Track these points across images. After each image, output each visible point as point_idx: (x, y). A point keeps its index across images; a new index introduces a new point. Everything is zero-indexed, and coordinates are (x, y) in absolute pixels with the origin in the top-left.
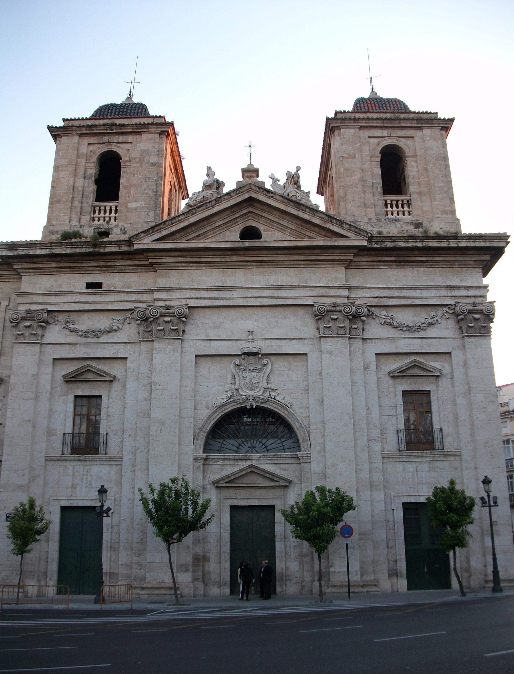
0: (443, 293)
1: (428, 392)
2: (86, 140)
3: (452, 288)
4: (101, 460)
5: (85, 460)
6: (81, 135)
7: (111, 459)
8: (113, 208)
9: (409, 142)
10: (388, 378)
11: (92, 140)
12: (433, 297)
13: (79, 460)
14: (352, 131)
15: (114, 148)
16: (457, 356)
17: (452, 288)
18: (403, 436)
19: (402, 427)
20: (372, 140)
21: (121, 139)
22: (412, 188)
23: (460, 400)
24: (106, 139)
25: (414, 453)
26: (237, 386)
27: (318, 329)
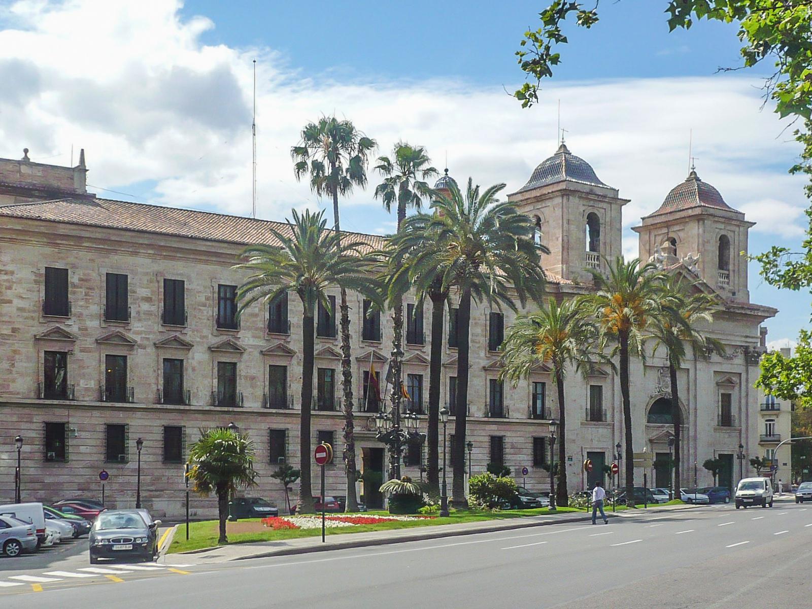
0: (743, 339)
1: (730, 395)
2: (582, 202)
3: (747, 337)
4: (604, 425)
5: (597, 425)
6: (580, 197)
7: (609, 425)
8: (596, 257)
9: (732, 234)
10: (715, 385)
11: (585, 203)
12: (739, 341)
13: (595, 425)
14: (710, 222)
15: (596, 212)
16: (744, 376)
17: (747, 337)
18: (720, 417)
19: (720, 413)
20: (717, 230)
21: (601, 205)
22: (731, 267)
23: (743, 401)
24: (591, 203)
25: (725, 428)
26: (661, 386)
27: (694, 355)
